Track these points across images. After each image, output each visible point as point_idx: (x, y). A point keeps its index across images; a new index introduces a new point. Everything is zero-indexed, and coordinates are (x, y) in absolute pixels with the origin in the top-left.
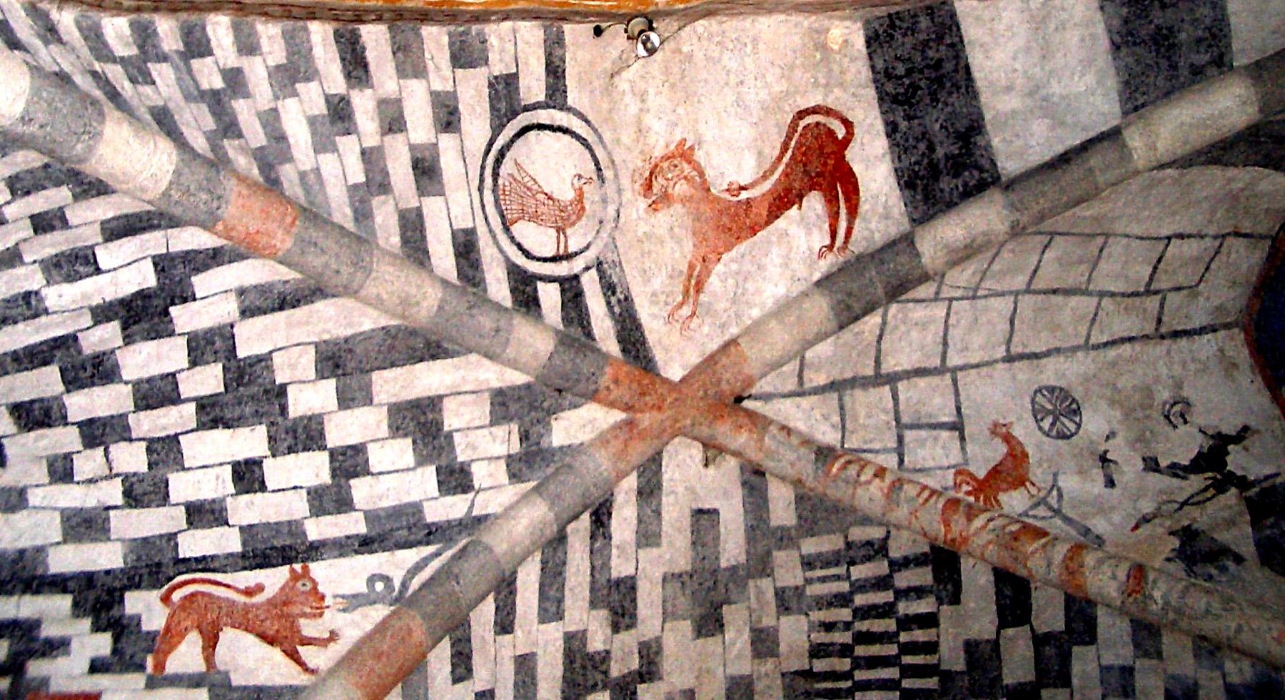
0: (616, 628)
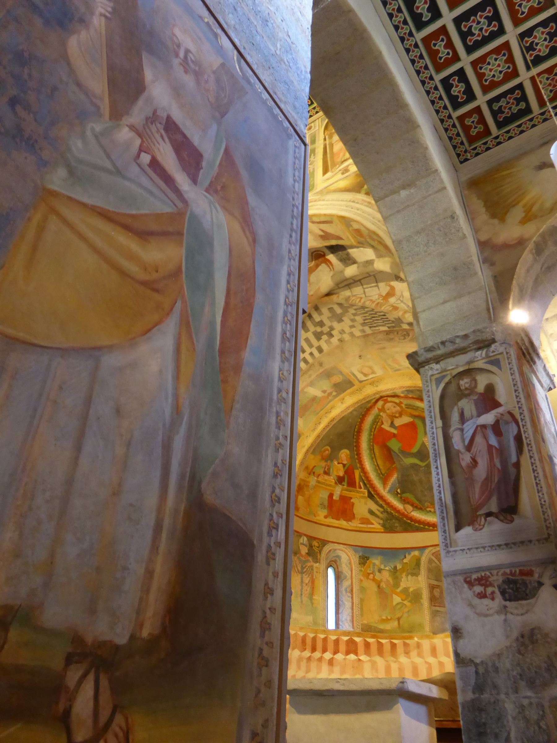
0: (322, 327)
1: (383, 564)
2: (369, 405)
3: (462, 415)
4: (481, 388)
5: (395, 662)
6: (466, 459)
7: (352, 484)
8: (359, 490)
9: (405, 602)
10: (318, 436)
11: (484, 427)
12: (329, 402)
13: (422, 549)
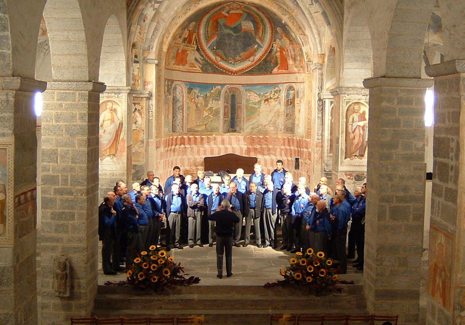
3: (353, 119)
4: (361, 112)
5: (202, 147)
6: (352, 136)
7: (190, 42)
9: (210, 115)
11: (360, 126)
13: (223, 85)
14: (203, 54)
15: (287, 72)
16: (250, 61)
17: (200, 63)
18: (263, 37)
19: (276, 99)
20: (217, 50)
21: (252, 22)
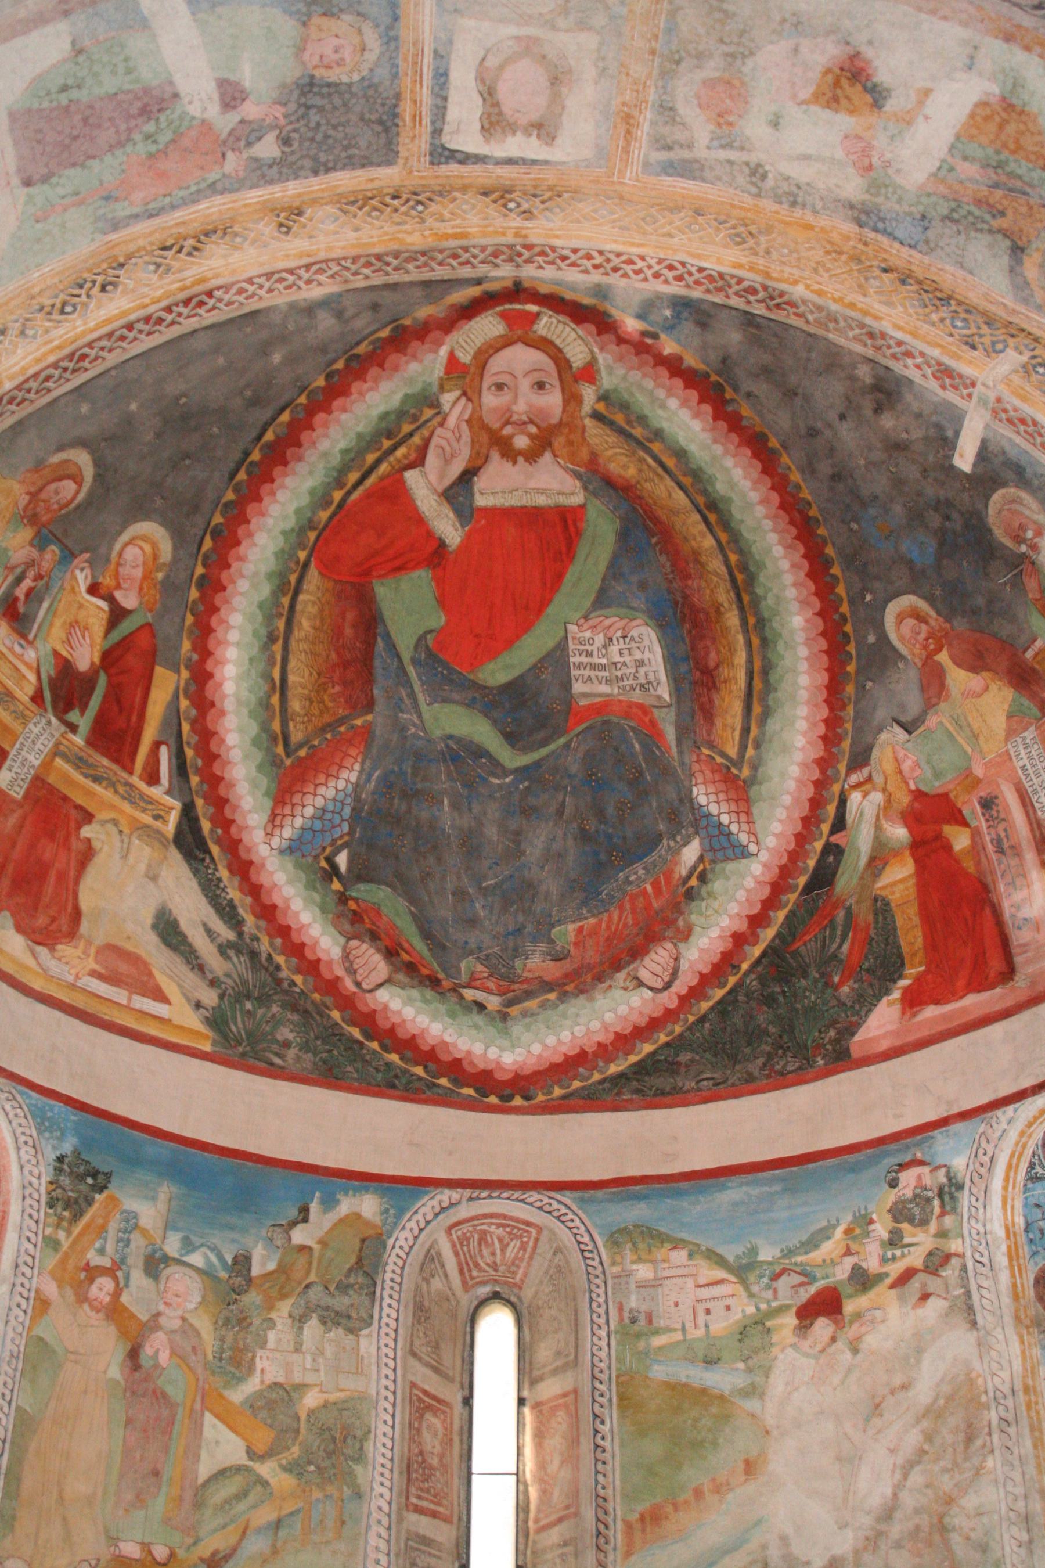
1: (176, 1229)
2: (423, 312)
8: (142, 786)
9: (265, 1469)
10: (78, 358)
12: (213, 189)
14: (233, 893)
15: (1009, 1002)
16: (640, 984)
17: (200, 968)
18: (750, 752)
19: (915, 1284)
20: (362, 887)
21: (662, 625)
